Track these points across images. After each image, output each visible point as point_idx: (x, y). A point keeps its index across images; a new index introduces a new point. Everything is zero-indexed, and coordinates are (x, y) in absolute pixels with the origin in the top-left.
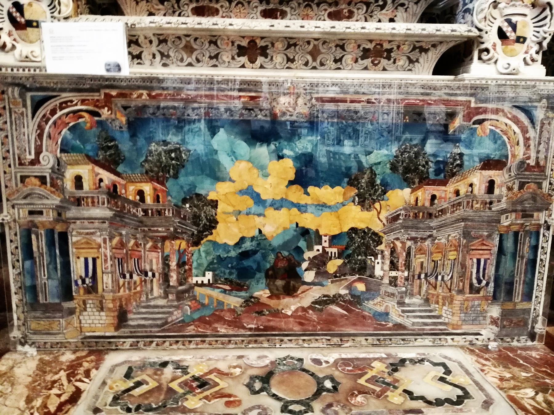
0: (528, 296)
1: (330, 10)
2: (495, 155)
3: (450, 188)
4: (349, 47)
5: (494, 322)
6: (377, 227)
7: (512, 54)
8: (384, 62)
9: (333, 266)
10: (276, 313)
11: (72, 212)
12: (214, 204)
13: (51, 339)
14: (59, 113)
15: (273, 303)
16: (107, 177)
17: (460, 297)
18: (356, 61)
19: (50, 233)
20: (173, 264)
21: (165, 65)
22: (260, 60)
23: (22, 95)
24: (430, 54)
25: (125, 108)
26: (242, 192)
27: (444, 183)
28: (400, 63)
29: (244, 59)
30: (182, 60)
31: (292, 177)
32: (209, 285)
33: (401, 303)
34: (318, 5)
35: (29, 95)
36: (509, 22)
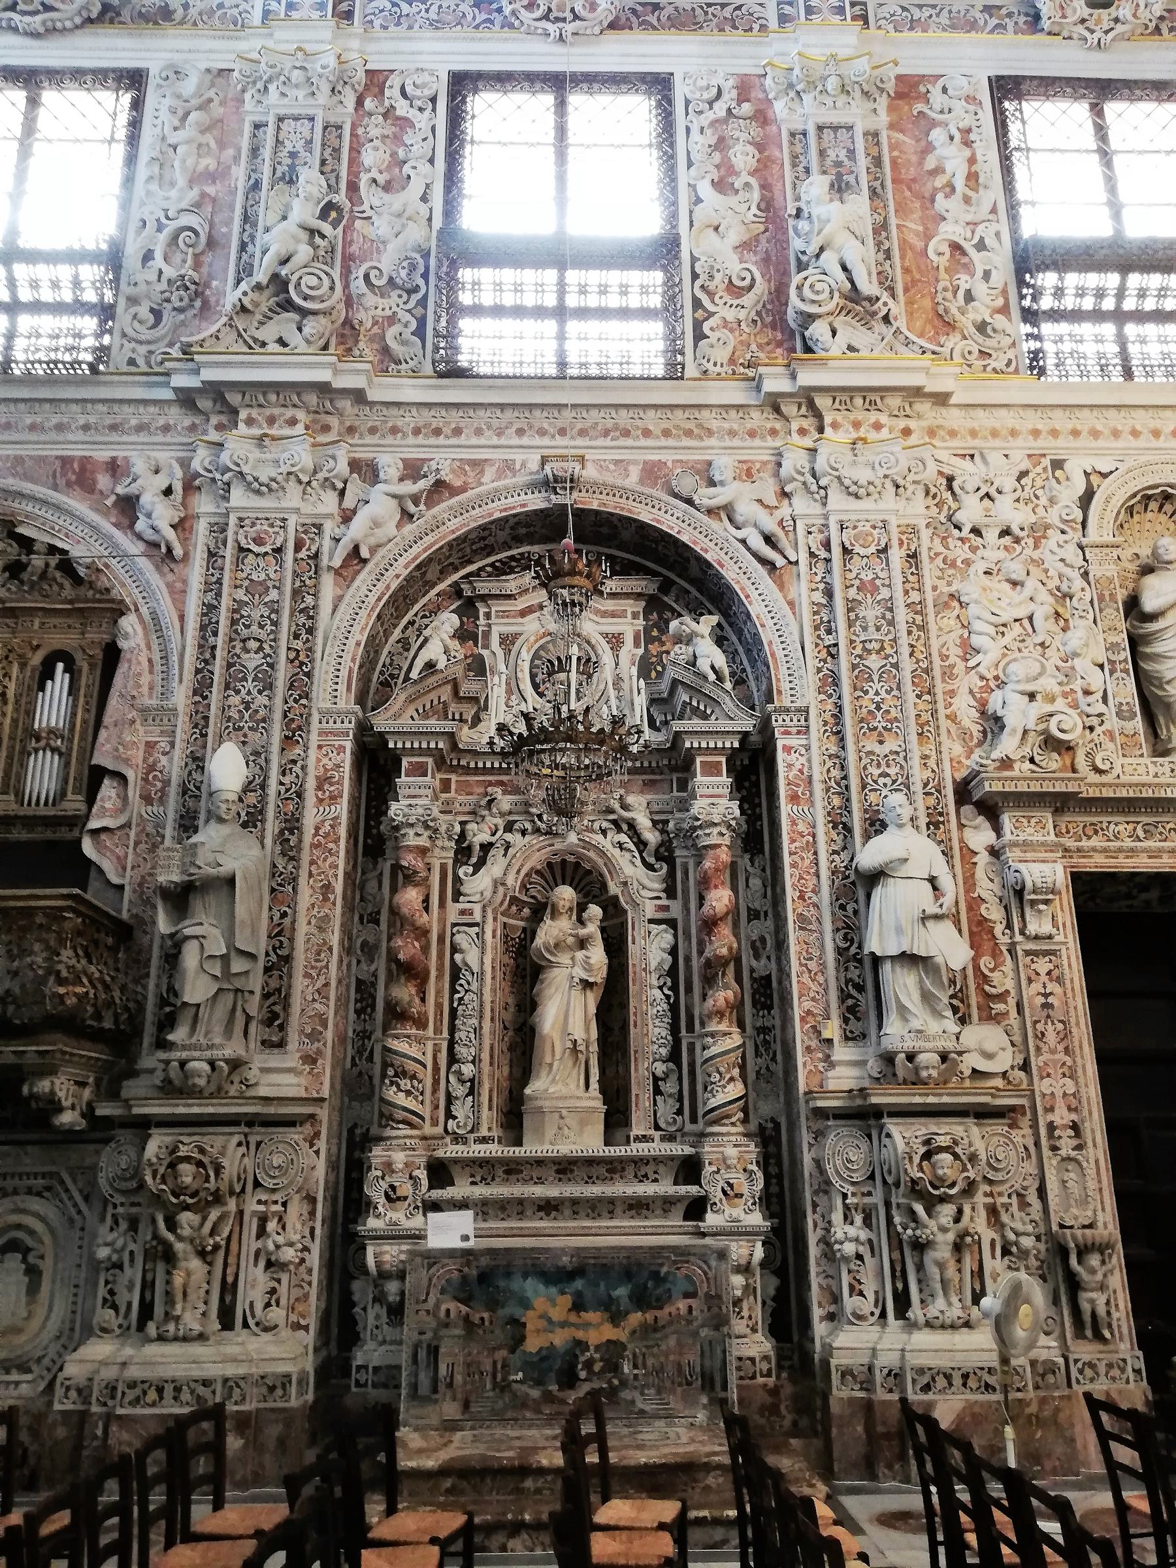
0: (725, 1387)
2: (691, 1289)
3: (667, 1310)
4: (618, 1203)
5: (705, 1407)
6: (624, 1339)
7: (735, 1206)
8: (645, 1212)
9: (597, 1367)
10: (563, 1402)
11: (443, 1332)
12: (524, 1325)
13: (423, 1422)
15: (561, 1395)
16: (464, 1309)
17: (679, 1389)
19: (429, 1346)
20: (499, 1366)
22: (554, 1214)
26: (541, 1317)
27: (661, 1308)
28: (658, 1212)
29: (542, 1214)
31: (570, 1305)
32: (521, 1382)
33: (642, 1394)
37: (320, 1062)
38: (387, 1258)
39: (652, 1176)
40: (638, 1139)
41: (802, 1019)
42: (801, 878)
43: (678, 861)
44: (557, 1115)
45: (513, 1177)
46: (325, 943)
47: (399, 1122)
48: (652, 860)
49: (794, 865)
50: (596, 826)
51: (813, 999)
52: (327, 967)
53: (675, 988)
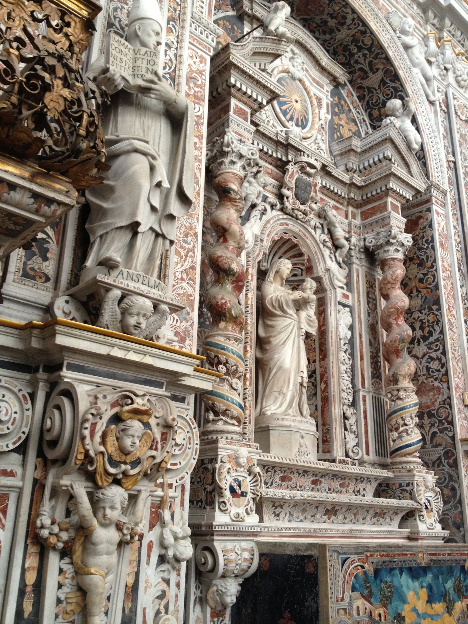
1: (341, 482)
14: (351, 567)
18: (371, 519)
21: (290, 521)
23: (338, 557)
24: (399, 515)
25: (373, 563)
29: (326, 517)
30: (298, 518)
34: (337, 479)
35: (341, 556)
36: (427, 499)
37: (187, 342)
38: (232, 556)
39: (362, 492)
40: (341, 462)
41: (456, 388)
42: (448, 297)
43: (355, 266)
44: (298, 435)
45: (285, 484)
46: (191, 228)
47: (233, 418)
48: (341, 260)
49: (445, 287)
50: (313, 223)
51: (458, 377)
52: (193, 250)
53: (352, 355)
